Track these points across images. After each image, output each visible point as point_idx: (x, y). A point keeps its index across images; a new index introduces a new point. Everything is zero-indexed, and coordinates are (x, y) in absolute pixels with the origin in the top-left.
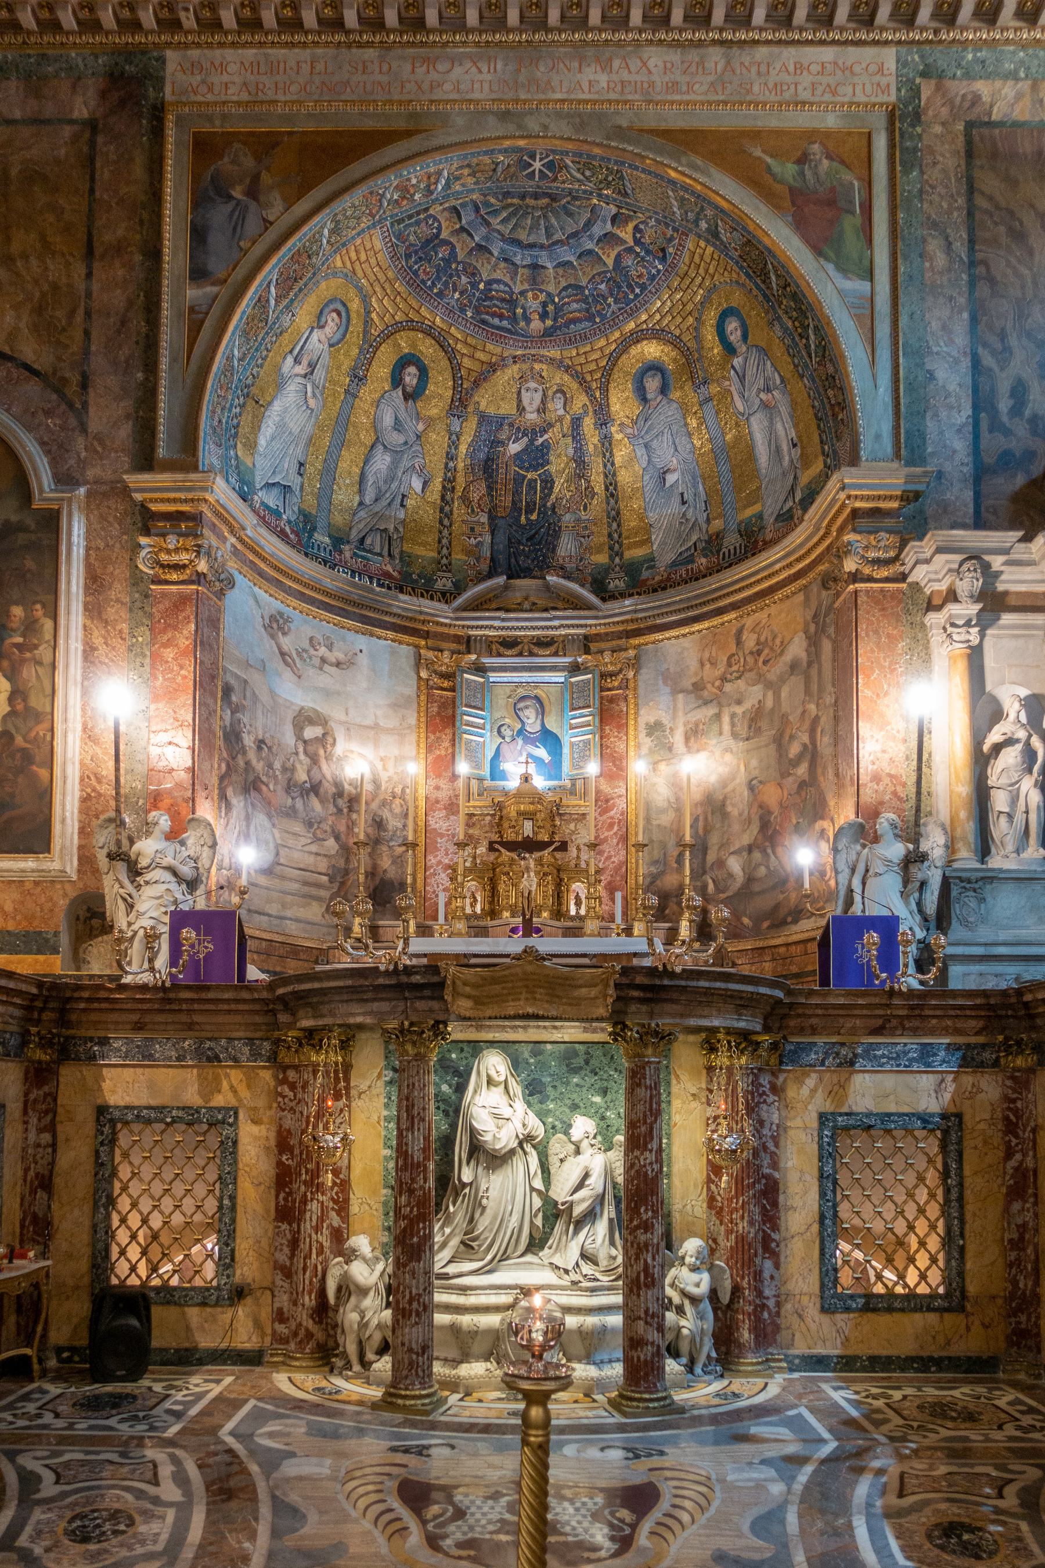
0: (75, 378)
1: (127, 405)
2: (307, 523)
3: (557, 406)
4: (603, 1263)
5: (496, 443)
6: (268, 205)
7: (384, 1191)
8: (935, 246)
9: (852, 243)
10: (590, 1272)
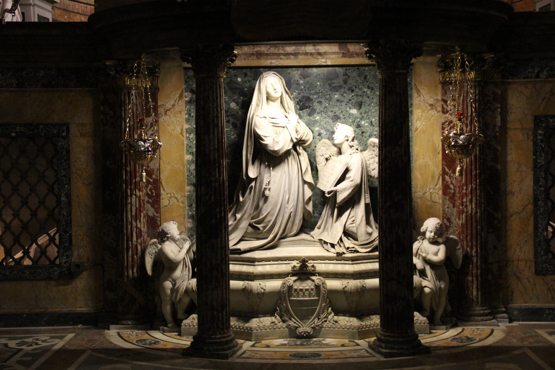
4: (362, 238)
7: (188, 188)
10: (352, 246)
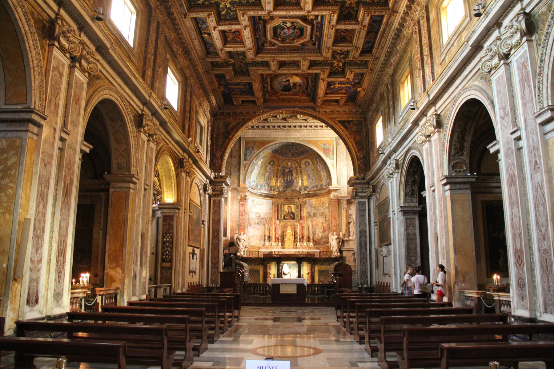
0: (229, 173)
1: (236, 177)
2: (257, 185)
3: (293, 165)
5: (284, 170)
6: (254, 151)
8: (342, 155)
9: (331, 155)
